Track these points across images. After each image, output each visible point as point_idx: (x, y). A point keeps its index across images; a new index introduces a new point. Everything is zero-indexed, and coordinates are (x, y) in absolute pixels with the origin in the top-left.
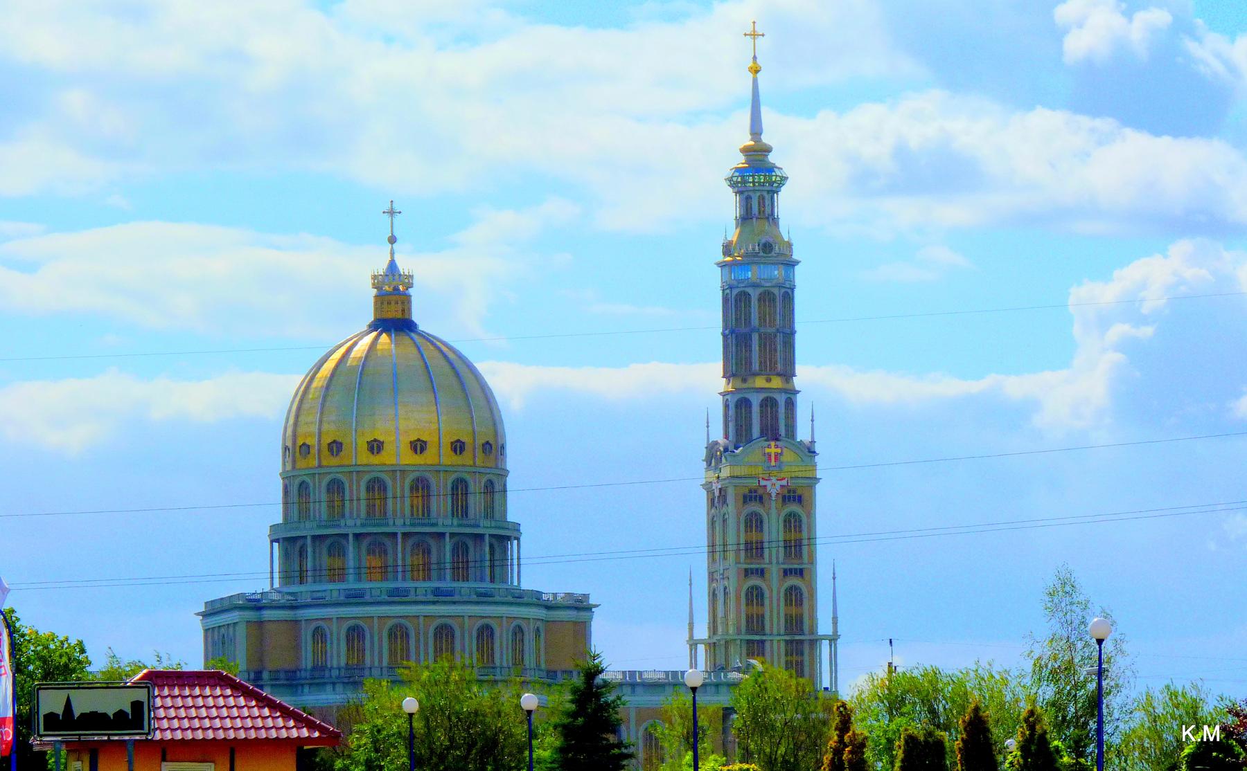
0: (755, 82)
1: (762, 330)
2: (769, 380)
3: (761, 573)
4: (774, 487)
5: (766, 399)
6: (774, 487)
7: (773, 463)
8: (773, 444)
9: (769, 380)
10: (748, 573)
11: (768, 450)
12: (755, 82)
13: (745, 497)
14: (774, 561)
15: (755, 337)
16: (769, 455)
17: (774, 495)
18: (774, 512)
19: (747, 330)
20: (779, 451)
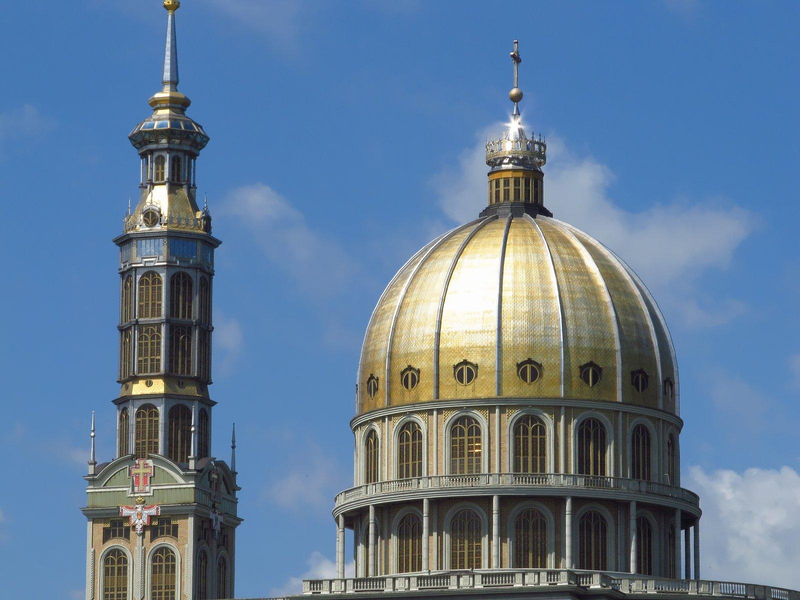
2: (149, 384)
4: (138, 517)
6: (138, 517)
9: (149, 384)
17: (139, 527)
18: (138, 549)
19: (156, 319)
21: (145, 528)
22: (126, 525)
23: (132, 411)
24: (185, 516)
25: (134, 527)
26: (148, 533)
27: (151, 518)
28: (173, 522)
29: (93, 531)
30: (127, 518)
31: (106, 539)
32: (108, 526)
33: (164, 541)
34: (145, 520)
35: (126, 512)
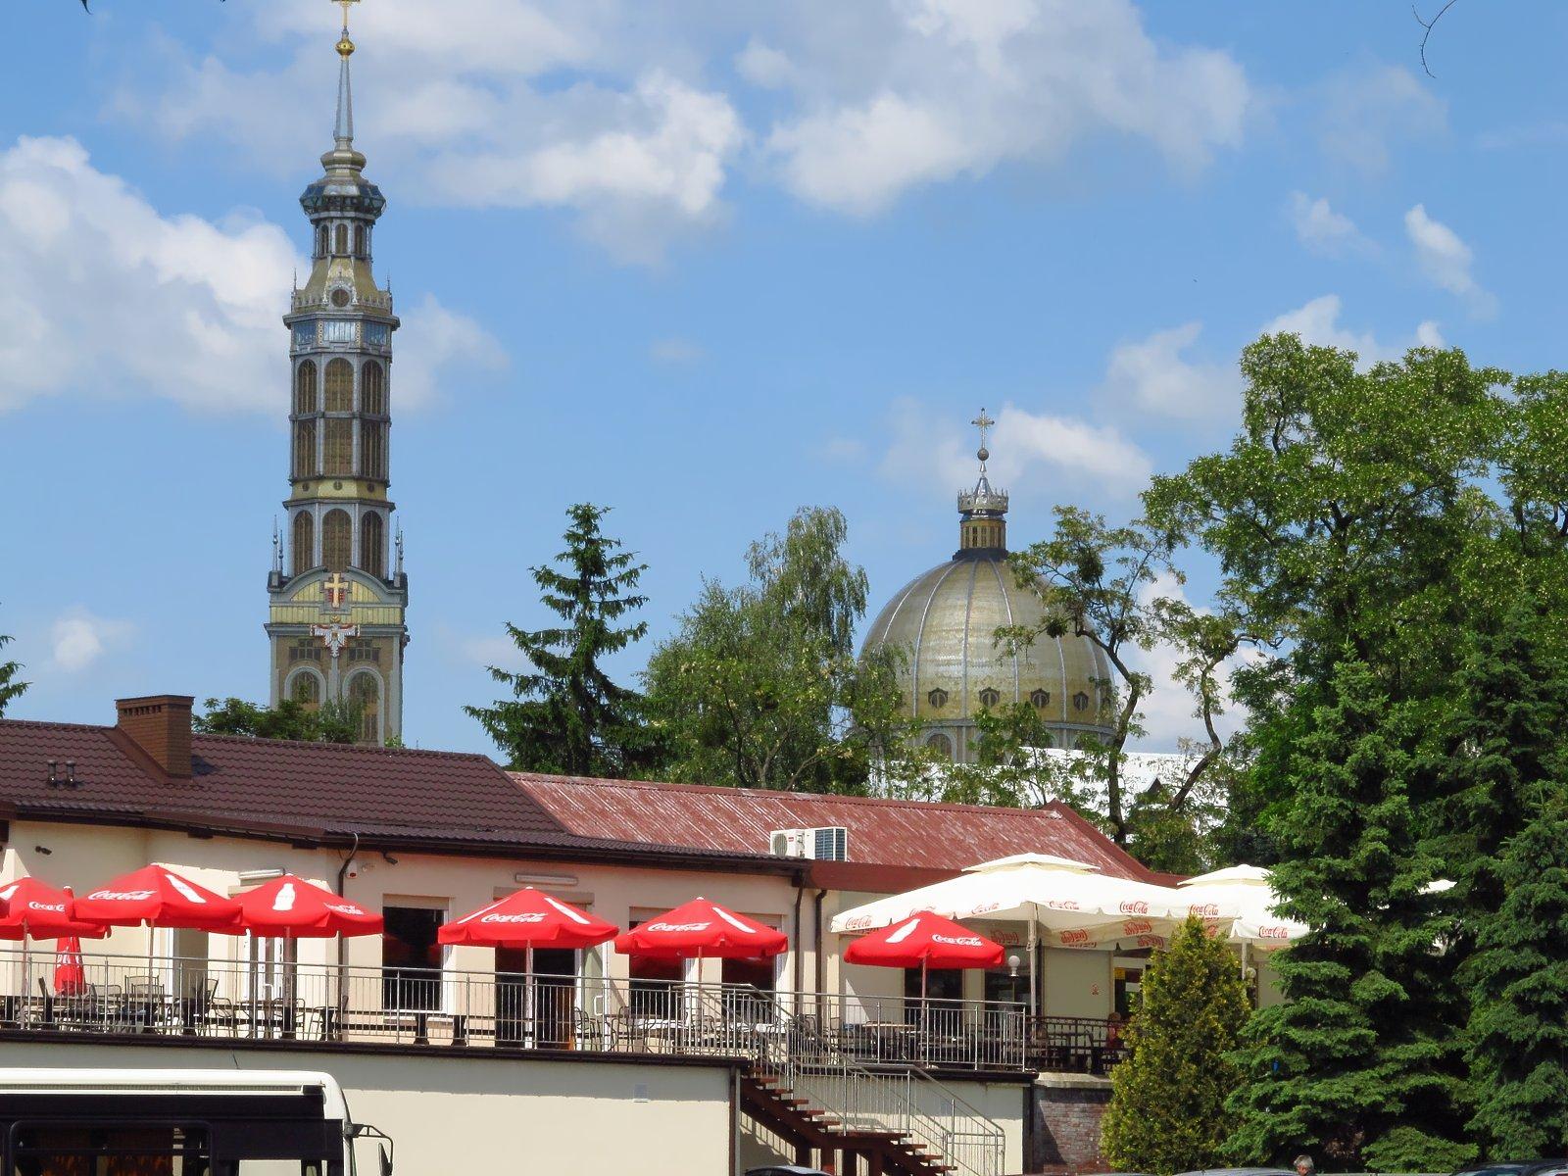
0: (345, 71)
1: (333, 414)
2: (338, 487)
4: (335, 639)
5: (333, 512)
6: (335, 639)
7: (336, 603)
8: (336, 576)
9: (338, 487)
11: (327, 585)
12: (345, 71)
15: (320, 424)
16: (331, 591)
19: (344, 414)
20: (345, 585)
21: (341, 649)
22: (316, 644)
23: (318, 514)
25: (329, 649)
26: (346, 656)
27: (348, 638)
28: (375, 644)
30: (321, 638)
32: (294, 643)
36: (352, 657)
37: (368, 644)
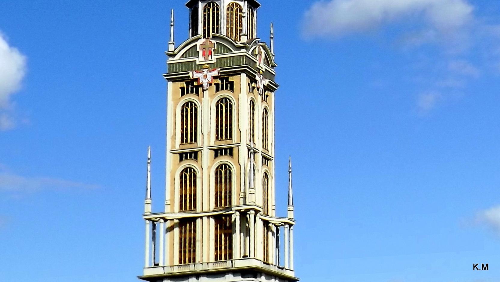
3: (195, 155)
6: (205, 78)
10: (183, 156)
13: (182, 89)
14: (206, 144)
21: (210, 85)
22: (195, 84)
24: (239, 73)
25: (201, 86)
27: (215, 78)
29: (173, 89)
30: (197, 80)
31: (183, 94)
33: (223, 93)
34: (209, 78)
35: (196, 75)
36: (217, 90)
37: (227, 79)
